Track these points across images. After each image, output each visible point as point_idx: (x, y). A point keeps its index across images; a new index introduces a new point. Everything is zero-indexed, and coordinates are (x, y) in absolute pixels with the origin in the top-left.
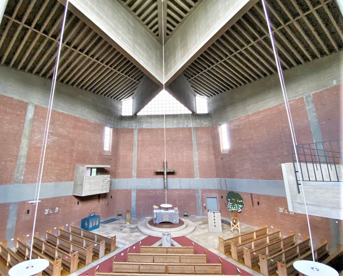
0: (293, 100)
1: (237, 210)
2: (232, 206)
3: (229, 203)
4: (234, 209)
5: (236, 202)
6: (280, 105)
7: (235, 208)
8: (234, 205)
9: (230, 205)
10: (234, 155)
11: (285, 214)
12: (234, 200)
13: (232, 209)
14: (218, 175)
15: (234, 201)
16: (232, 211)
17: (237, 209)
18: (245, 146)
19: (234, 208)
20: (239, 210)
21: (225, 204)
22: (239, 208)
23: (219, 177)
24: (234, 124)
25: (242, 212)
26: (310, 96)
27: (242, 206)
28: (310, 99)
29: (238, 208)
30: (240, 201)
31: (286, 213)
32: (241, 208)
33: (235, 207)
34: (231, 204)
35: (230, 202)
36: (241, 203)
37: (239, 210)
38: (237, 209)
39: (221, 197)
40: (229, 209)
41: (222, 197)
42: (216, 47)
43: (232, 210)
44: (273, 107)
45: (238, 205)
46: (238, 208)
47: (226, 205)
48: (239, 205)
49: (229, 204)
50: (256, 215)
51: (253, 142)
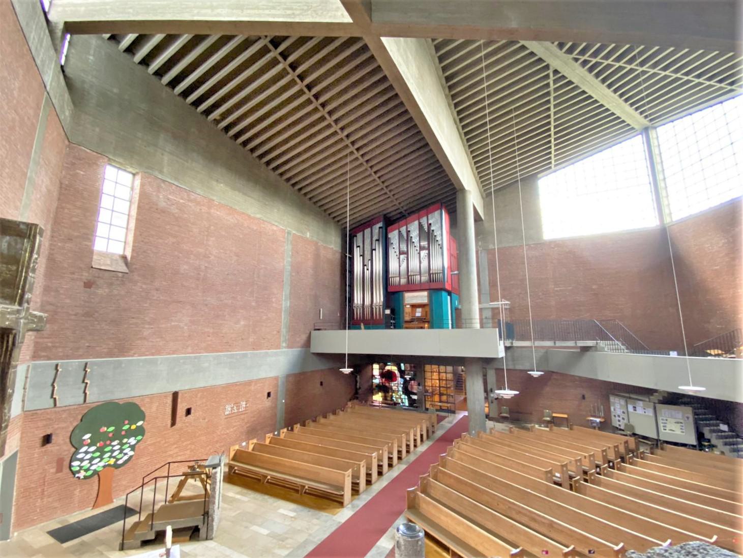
0: (276, 226)
1: (118, 460)
2: (98, 454)
3: (84, 449)
4: (102, 464)
5: (118, 436)
6: (262, 221)
7: (110, 457)
8: (109, 448)
9: (89, 456)
10: (145, 284)
11: (235, 414)
12: (111, 429)
13: (93, 468)
14: (46, 349)
15: (111, 435)
16: (96, 473)
17: (114, 457)
18: (186, 267)
19: (102, 459)
20: (126, 454)
21: (60, 462)
22: (127, 450)
23: (49, 358)
24: (170, 197)
25: (133, 458)
26: (290, 234)
27: (139, 438)
28: (290, 238)
29: (121, 450)
30: (133, 427)
31: (234, 413)
32: (133, 448)
33: (108, 454)
34: (93, 449)
35: (89, 445)
36: (140, 431)
37: (126, 454)
38: (114, 457)
39: (38, 441)
40: (78, 472)
41: (47, 439)
42: (420, 140)
43: (89, 473)
44: (254, 218)
45: (125, 441)
46: (121, 450)
47: (65, 465)
48: (129, 438)
49: (80, 456)
50: (175, 446)
51: (206, 265)
